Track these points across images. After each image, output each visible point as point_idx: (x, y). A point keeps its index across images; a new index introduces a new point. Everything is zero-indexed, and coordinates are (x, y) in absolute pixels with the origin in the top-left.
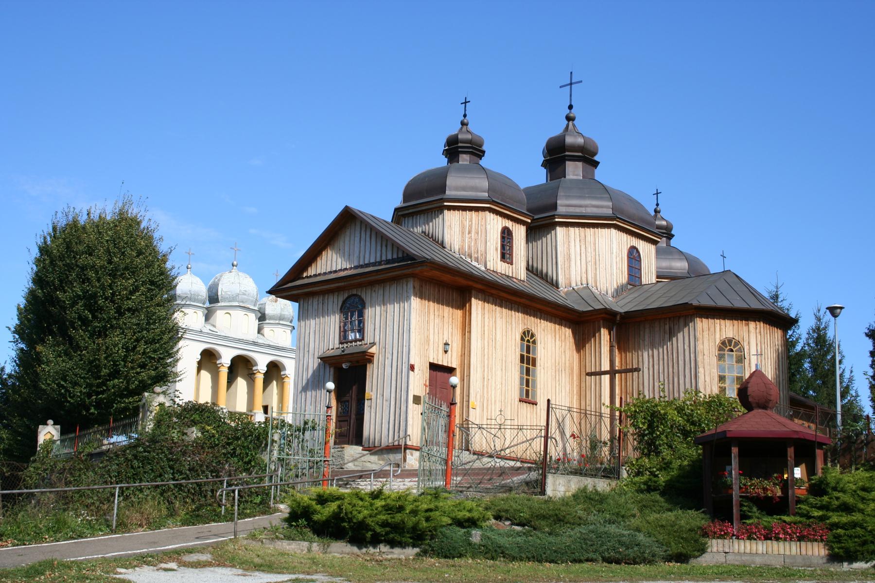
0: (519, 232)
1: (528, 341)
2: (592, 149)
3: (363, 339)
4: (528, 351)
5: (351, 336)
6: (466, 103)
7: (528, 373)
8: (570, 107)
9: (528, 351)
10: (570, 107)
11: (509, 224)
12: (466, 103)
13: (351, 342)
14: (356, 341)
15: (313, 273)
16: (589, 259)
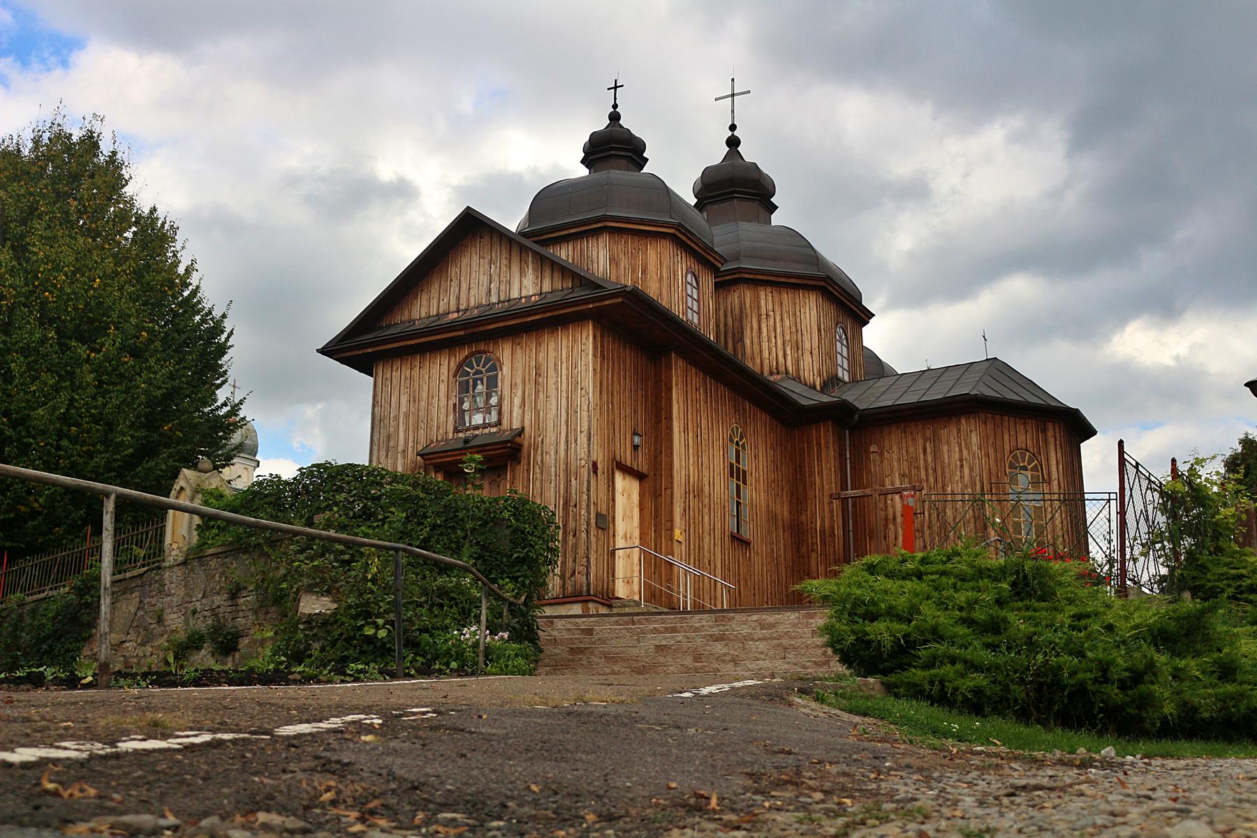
0: (708, 281)
1: (737, 443)
2: (770, 189)
3: (499, 422)
4: (738, 461)
5: (478, 419)
6: (616, 87)
7: (738, 496)
8: (733, 127)
9: (738, 461)
10: (733, 127)
11: (695, 267)
12: (616, 87)
13: (477, 428)
14: (485, 426)
15: (405, 318)
16: (788, 338)
